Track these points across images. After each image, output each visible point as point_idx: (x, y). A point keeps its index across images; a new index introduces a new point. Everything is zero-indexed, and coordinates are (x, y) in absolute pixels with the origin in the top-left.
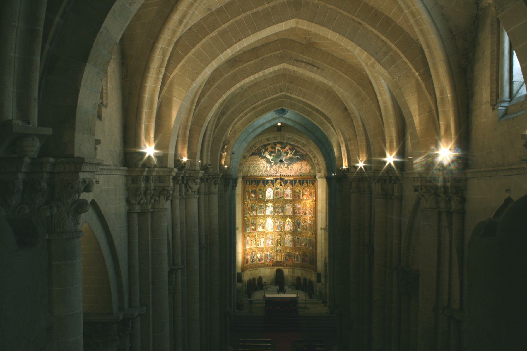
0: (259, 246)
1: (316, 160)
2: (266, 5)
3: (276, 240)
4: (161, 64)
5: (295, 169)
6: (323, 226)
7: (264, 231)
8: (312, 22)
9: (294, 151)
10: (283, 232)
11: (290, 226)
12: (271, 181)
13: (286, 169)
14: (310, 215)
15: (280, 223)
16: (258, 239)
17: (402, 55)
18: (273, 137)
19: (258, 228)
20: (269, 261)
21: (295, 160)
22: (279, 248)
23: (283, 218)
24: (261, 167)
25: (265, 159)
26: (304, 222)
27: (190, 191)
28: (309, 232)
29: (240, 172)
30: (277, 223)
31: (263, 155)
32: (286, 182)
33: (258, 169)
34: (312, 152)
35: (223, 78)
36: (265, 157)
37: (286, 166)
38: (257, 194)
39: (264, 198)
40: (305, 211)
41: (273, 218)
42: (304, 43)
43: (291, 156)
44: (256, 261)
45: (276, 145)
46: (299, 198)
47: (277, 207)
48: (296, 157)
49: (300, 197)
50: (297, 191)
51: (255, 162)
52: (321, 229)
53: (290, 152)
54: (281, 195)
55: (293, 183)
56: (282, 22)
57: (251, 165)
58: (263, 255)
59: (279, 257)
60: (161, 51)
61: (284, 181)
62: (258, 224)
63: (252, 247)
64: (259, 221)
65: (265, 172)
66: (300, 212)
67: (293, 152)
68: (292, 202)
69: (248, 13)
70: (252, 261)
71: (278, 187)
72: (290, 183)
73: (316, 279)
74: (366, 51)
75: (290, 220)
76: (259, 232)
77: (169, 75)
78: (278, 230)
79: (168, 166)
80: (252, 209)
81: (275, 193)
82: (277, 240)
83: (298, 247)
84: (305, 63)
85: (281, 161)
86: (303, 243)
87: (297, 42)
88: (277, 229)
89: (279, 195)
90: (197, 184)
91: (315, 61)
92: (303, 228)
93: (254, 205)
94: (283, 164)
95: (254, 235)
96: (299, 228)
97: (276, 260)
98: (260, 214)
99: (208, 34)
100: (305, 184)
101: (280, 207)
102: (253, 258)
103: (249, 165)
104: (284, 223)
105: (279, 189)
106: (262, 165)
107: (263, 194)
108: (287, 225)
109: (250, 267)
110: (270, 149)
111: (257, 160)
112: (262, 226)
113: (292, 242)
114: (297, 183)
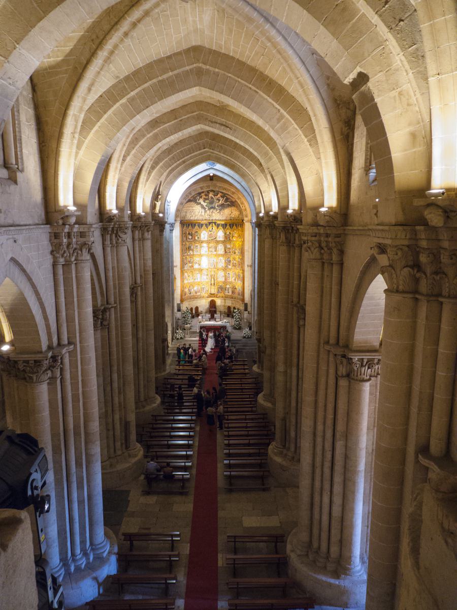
0: (196, 281)
2: (171, 74)
4: (74, 130)
6: (250, 264)
8: (213, 90)
17: (293, 122)
18: (206, 186)
27: (120, 240)
32: (218, 226)
34: (240, 199)
35: (146, 138)
36: (200, 203)
37: (218, 211)
42: (218, 105)
44: (193, 293)
45: (209, 193)
46: (230, 240)
50: (228, 233)
52: (248, 266)
53: (221, 199)
55: (224, 226)
56: (186, 90)
60: (74, 117)
69: (155, 81)
73: (244, 308)
74: (261, 117)
75: (222, 258)
77: (84, 139)
79: (88, 223)
80: (189, 249)
84: (219, 124)
86: (233, 278)
87: (211, 104)
90: (126, 233)
91: (228, 122)
99: (118, 101)
100: (235, 227)
106: (197, 210)
114: (228, 226)
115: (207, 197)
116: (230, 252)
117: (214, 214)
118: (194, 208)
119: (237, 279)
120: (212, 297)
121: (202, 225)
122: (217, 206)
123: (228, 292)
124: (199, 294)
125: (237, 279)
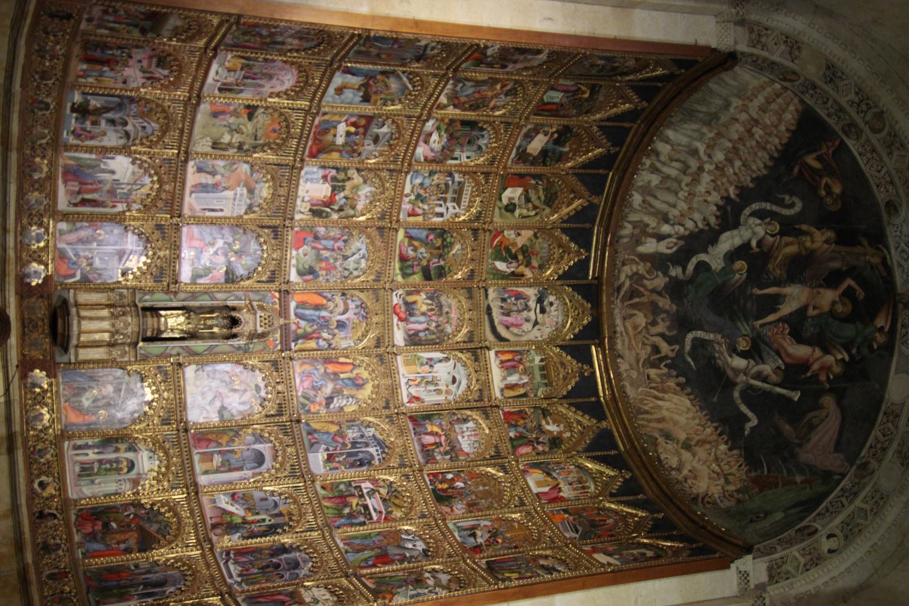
1: (832, 544)
3: (230, 303)
5: (660, 407)
7: (298, 217)
9: (796, 396)
10: (286, 347)
11: (329, 400)
12: (588, 259)
13: (644, 354)
14: (459, 539)
15: (341, 325)
16: (246, 167)
19: (321, 172)
20: (62, 256)
21: (715, 399)
22: (171, 322)
23: (378, 346)
24: (671, 198)
25: (713, 221)
26: (384, 491)
28: (341, 545)
29: (754, 36)
30: (341, 308)
31: (747, 211)
33: (668, 177)
37: (665, 348)
38: (538, 170)
39: (497, 219)
40: (461, 494)
41: (373, 277)
43: (742, 378)
47: (440, 307)
48: (744, 408)
49: (524, 450)
50: (552, 428)
51: (719, 156)
53: (767, 369)
54: (507, 327)
57: (711, 135)
58: (120, 207)
59: (106, 325)
61: (585, 342)
62: (352, 173)
63: (205, 108)
64: (365, 182)
65: (635, 225)
66: (439, 457)
67: (779, 385)
68: (481, 399)
70: (82, 111)
71: (551, 304)
72: (581, 374)
75: (368, 390)
76: (293, 182)
78: (296, 315)
81: (520, 289)
82: (227, 307)
83: (198, 468)
85: (683, 324)
86: (233, 496)
88: (302, 305)
89: (508, 315)
92: (342, 487)
93: (480, 148)
94: (674, 332)
95: (289, 136)
96: (330, 458)
97: (77, 305)
98: (407, 190)
101: (437, 327)
102: (112, 122)
103: (724, 119)
104: (347, 357)
105: (543, 311)
106: (683, 206)
107: (525, 212)
108: (335, 374)
109: (44, 76)
110: (792, 249)
111: (723, 175)
112: (329, 203)
113: (221, 414)
115: (775, 268)
116: (428, 453)
117: (641, 319)
118: (706, 178)
119: (232, 541)
120: (25, 324)
121: (582, 238)
122: (699, 344)
123: (86, 471)
124: (63, 202)
125: (232, 541)
